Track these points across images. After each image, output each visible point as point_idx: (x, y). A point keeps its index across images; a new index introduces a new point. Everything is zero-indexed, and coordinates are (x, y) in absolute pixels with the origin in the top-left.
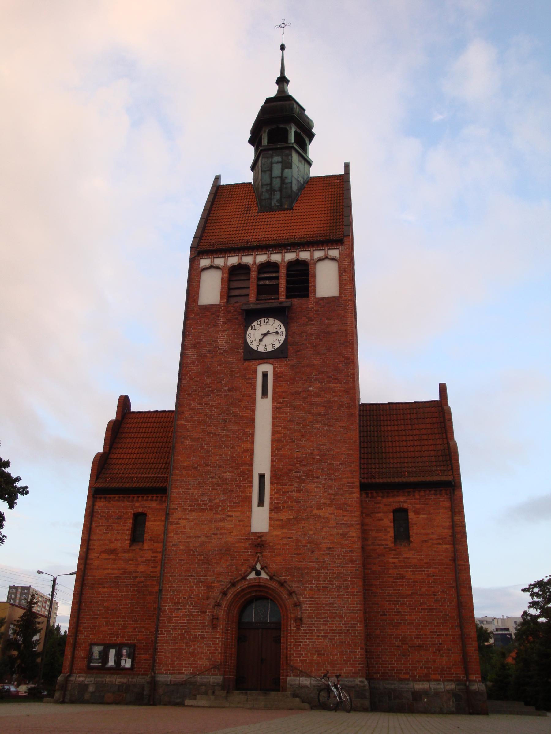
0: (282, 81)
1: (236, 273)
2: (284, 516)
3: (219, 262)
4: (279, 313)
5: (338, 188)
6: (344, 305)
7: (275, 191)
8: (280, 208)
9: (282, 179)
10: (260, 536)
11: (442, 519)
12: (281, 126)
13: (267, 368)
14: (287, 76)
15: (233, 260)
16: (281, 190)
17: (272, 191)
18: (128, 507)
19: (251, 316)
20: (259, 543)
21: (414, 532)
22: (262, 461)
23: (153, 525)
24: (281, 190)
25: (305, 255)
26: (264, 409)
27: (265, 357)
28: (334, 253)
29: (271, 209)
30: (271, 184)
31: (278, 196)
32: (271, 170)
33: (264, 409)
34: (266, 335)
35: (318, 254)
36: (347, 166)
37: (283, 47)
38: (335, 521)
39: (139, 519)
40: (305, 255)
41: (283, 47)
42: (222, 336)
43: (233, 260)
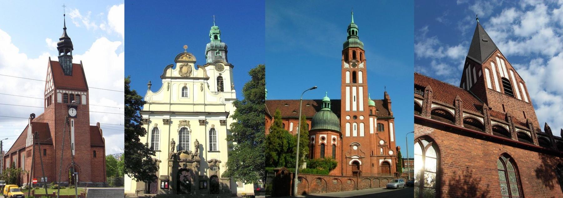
1: (65, 96)
2: (78, 152)
3: (61, 91)
4: (76, 108)
6: (87, 107)
8: (69, 75)
11: (102, 153)
12: (65, 45)
13: (72, 120)
15: (64, 92)
17: (67, 69)
18: (43, 147)
19: (69, 107)
20: (73, 157)
21: (97, 155)
22: (73, 141)
23: (48, 152)
25: (79, 93)
27: (73, 117)
28: (85, 93)
29: (66, 74)
31: (68, 71)
34: (73, 112)
35: (82, 93)
36: (81, 62)
38: (87, 154)
39: (45, 150)
42: (64, 112)
43: (64, 92)
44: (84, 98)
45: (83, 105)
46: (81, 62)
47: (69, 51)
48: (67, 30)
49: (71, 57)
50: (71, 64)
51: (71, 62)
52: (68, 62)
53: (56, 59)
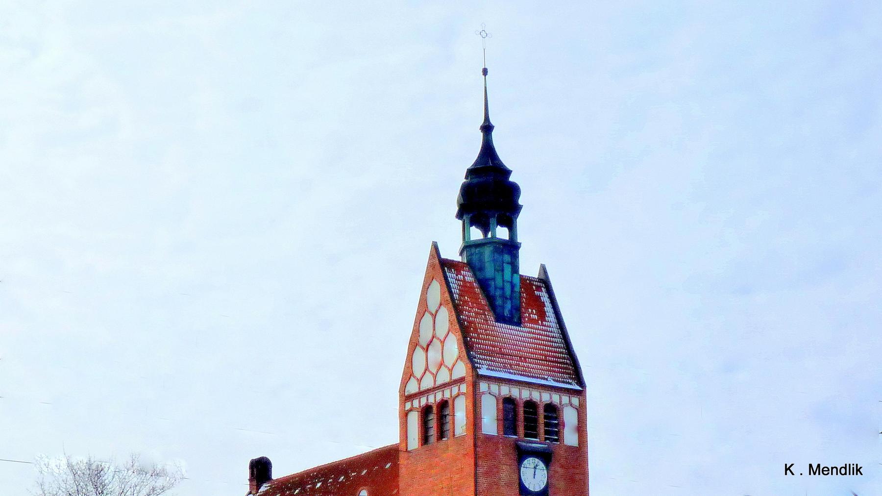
0: (487, 128)
3: (494, 388)
4: (546, 457)
6: (579, 454)
7: (507, 298)
14: (493, 121)
15: (505, 391)
16: (511, 299)
17: (503, 296)
19: (522, 454)
24: (511, 299)
25: (556, 398)
28: (575, 401)
30: (503, 289)
31: (508, 306)
32: (503, 270)
35: (565, 399)
37: (485, 72)
41: (485, 72)
43: (505, 391)
44: (569, 417)
46: (544, 269)
48: (493, 133)
49: (511, 248)
50: (516, 280)
51: (515, 269)
52: (508, 269)
53: (452, 252)
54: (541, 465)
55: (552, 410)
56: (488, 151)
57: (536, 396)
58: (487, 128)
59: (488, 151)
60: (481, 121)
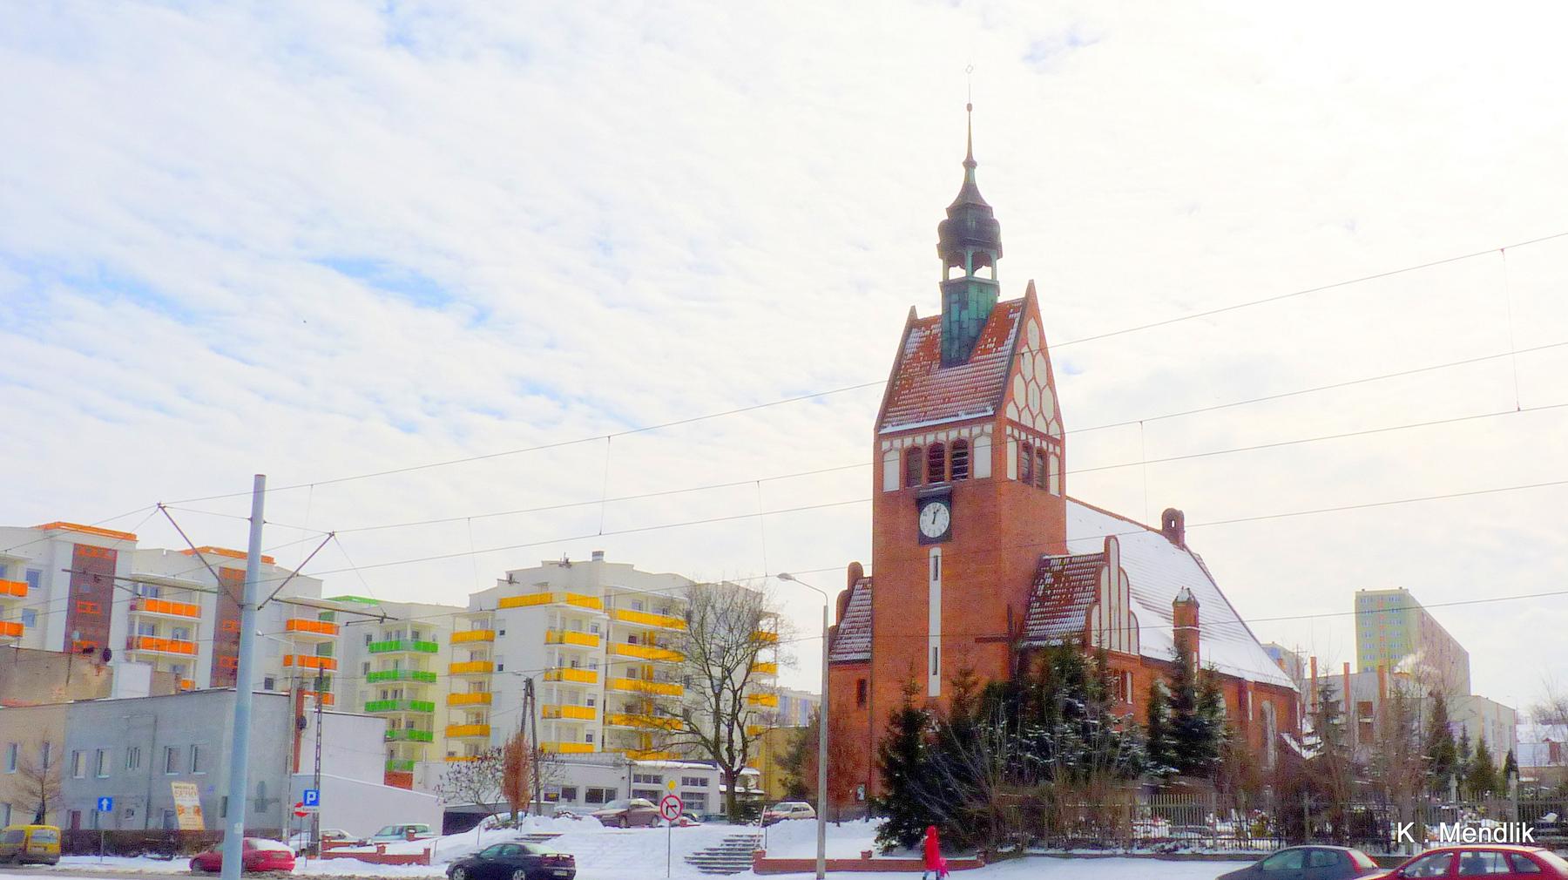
0: (970, 164)
3: (897, 443)
5: (1027, 306)
9: (960, 322)
10: (934, 699)
12: (969, 233)
13: (936, 551)
14: (975, 158)
19: (921, 503)
25: (965, 433)
26: (935, 588)
28: (989, 428)
31: (956, 346)
33: (935, 588)
34: (935, 520)
35: (976, 430)
37: (969, 107)
40: (965, 433)
41: (969, 107)
43: (908, 442)
45: (984, 483)
46: (1031, 288)
47: (988, 261)
48: (977, 171)
54: (943, 508)
55: (962, 450)
56: (969, 188)
57: (942, 437)
58: (970, 164)
59: (969, 188)
60: (964, 158)
